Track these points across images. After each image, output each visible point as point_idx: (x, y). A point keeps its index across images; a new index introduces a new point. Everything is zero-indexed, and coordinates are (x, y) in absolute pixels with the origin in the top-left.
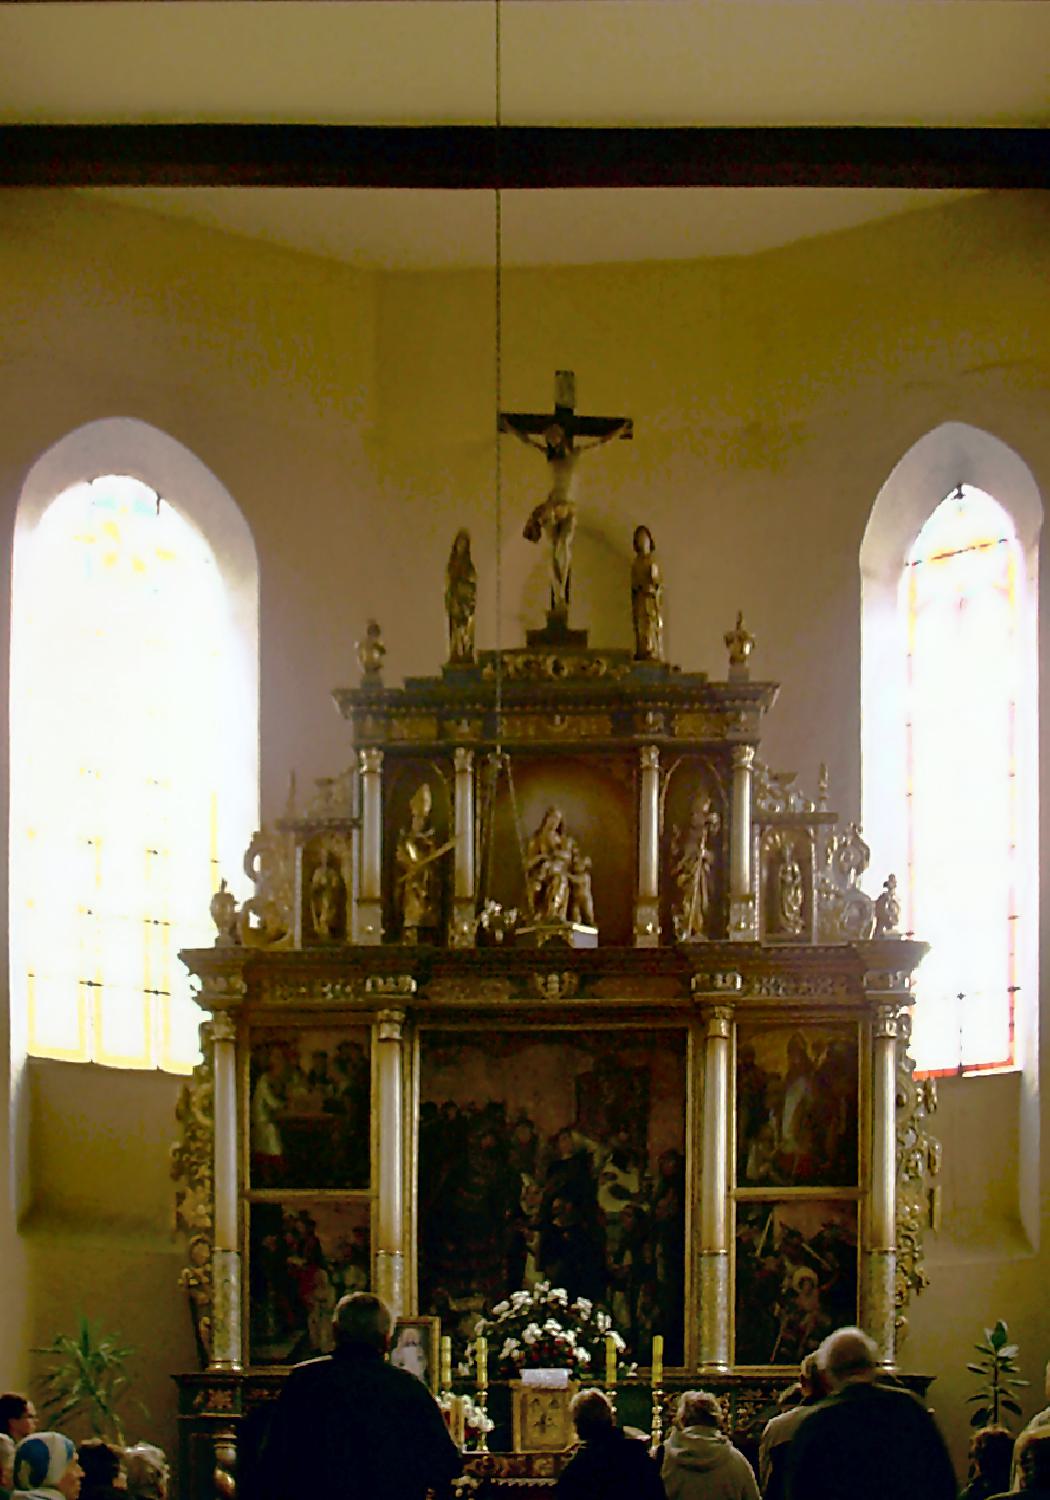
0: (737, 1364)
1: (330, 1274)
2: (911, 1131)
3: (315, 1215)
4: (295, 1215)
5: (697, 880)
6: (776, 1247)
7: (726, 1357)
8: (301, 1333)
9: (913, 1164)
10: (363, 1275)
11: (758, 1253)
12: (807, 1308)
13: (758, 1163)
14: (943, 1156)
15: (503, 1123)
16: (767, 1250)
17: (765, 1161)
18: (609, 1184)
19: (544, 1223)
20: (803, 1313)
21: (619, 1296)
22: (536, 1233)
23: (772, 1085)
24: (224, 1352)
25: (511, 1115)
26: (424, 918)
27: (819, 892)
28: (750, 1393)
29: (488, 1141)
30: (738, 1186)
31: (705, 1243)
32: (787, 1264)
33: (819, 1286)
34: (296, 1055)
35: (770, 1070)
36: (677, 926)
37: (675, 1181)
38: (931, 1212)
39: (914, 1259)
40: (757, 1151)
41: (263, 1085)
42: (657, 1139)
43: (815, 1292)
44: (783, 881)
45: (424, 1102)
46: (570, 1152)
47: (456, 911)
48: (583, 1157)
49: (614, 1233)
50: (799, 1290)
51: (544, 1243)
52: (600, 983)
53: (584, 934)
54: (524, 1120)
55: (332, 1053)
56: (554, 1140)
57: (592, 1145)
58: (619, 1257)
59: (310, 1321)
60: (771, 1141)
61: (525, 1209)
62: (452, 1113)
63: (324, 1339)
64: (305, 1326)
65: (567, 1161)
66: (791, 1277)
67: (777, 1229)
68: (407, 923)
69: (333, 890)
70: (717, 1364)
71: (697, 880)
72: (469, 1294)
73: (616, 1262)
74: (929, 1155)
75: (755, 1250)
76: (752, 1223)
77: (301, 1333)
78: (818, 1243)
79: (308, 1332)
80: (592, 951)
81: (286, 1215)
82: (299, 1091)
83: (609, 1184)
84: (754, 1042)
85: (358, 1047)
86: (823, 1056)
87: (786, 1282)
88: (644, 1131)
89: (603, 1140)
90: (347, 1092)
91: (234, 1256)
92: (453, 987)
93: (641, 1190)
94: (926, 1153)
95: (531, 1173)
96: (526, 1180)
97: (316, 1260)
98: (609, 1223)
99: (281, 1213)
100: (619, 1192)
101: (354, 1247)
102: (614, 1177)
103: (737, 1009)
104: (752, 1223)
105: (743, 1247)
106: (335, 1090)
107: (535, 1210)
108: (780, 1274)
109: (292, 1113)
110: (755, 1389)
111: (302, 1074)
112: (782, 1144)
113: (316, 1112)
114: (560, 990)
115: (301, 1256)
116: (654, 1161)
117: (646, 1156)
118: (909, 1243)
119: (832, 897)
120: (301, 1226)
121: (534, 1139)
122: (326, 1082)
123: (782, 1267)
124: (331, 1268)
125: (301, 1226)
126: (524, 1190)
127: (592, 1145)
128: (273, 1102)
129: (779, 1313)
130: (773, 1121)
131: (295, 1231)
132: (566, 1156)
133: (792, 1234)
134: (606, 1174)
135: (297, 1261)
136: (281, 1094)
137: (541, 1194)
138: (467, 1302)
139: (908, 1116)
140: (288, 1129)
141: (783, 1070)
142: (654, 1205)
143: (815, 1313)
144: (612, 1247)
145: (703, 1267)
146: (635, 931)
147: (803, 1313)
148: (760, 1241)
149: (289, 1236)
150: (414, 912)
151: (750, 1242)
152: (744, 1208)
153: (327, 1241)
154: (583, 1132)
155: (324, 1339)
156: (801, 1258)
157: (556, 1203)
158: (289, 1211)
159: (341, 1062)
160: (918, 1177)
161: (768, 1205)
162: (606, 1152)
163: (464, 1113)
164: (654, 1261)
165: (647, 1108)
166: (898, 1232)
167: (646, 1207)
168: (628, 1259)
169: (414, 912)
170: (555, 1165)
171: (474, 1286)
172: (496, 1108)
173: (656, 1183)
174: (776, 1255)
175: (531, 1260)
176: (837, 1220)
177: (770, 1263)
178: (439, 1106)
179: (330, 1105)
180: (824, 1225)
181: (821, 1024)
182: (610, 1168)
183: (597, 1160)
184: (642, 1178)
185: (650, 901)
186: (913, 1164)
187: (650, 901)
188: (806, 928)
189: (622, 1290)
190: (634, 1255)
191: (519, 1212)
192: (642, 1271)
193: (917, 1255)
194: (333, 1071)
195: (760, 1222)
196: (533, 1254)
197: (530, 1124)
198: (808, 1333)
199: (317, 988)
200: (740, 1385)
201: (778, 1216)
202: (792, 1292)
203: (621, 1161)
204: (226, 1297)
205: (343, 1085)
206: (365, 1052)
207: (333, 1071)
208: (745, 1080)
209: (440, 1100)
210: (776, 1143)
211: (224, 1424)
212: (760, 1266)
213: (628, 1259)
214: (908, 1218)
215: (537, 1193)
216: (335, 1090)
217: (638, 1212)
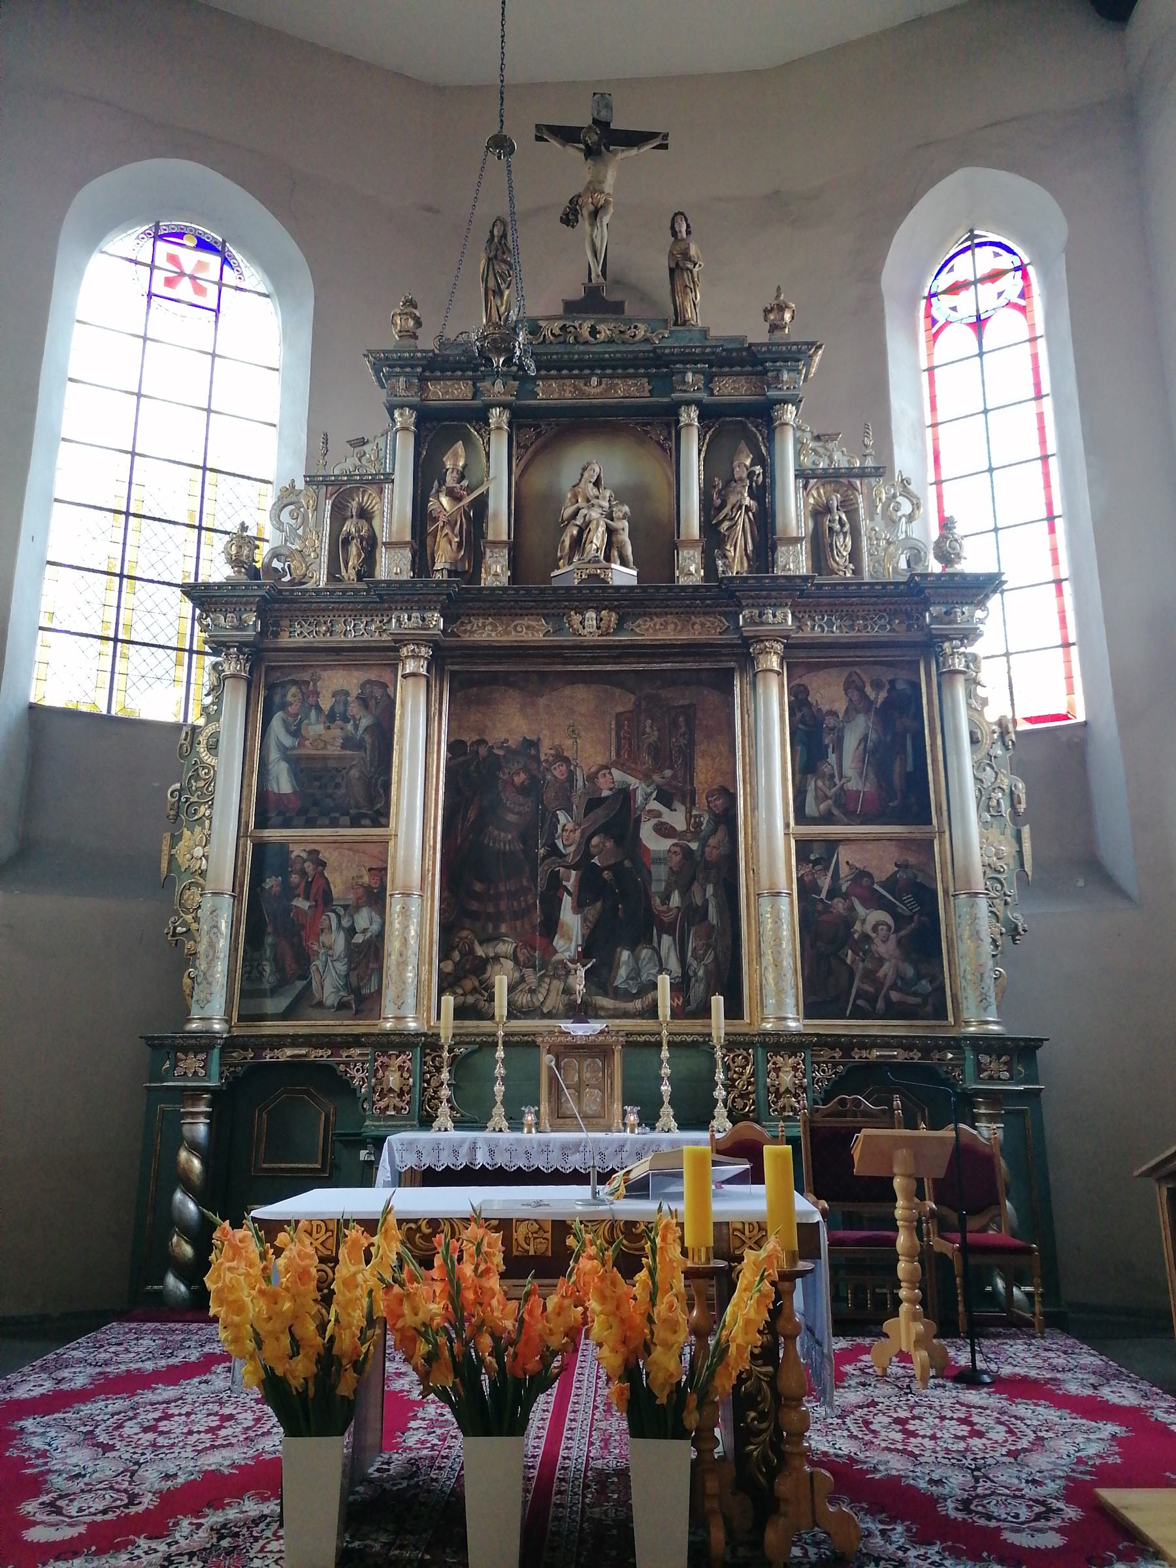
0: (807, 1017)
1: (339, 917)
2: (988, 768)
3: (325, 855)
4: (304, 855)
5: (740, 527)
6: (844, 888)
7: (794, 1010)
8: (300, 984)
9: (994, 803)
10: (377, 918)
11: (823, 896)
12: (886, 956)
13: (819, 799)
14: (1027, 794)
15: (536, 758)
16: (833, 893)
17: (826, 797)
18: (654, 821)
19: (584, 863)
20: (881, 961)
21: (666, 940)
22: (573, 873)
23: (829, 721)
24: (202, 1008)
25: (545, 751)
26: (454, 563)
27: (870, 538)
28: (825, 1054)
29: (521, 778)
30: (797, 823)
31: (765, 882)
32: (860, 909)
33: (897, 931)
34: (317, 694)
35: (825, 708)
36: (720, 569)
37: (726, 819)
38: (1020, 853)
39: (1006, 903)
40: (816, 787)
41: (277, 722)
42: (704, 775)
43: (893, 937)
44: (831, 529)
45: (452, 739)
46: (611, 789)
47: (488, 553)
48: (625, 795)
49: (660, 873)
50: (873, 935)
51: (582, 883)
52: (640, 621)
53: (623, 575)
54: (560, 757)
55: (355, 692)
56: (592, 778)
57: (634, 782)
58: (666, 898)
59: (313, 968)
60: (832, 776)
61: (561, 847)
62: (483, 751)
63: (328, 989)
64: (304, 975)
65: (607, 798)
66: (864, 921)
67: (844, 871)
68: (438, 566)
69: (362, 538)
70: (785, 1019)
71: (740, 527)
72: (496, 938)
73: (663, 903)
74: (1012, 792)
75: (819, 892)
76: (816, 862)
77: (300, 984)
78: (891, 884)
79: (310, 983)
80: (631, 588)
81: (293, 855)
82: (315, 728)
83: (654, 821)
84: (805, 680)
85: (384, 686)
86: (883, 695)
87: (857, 926)
88: (689, 767)
89: (646, 777)
90: (366, 729)
91: (226, 902)
92: (484, 626)
93: (688, 828)
94: (1007, 791)
95: (569, 810)
96: (562, 817)
97: (325, 899)
98: (659, 861)
99: (290, 852)
100: (664, 830)
101: (368, 889)
102: (659, 814)
103: (786, 646)
104: (816, 862)
105: (806, 889)
106: (356, 727)
107: (572, 849)
108: (848, 921)
109: (308, 750)
110: (833, 1049)
111: (319, 709)
112: (843, 780)
113: (334, 750)
114: (598, 628)
115: (307, 898)
116: (701, 799)
117: (693, 792)
118: (999, 887)
119: (883, 543)
120: (309, 867)
121: (571, 775)
122: (346, 720)
123: (852, 909)
124: (342, 912)
125: (309, 867)
126: (560, 828)
127: (634, 782)
128: (288, 741)
129: (853, 961)
130: (832, 758)
131: (303, 873)
132: (605, 793)
133: (861, 875)
134: (650, 811)
135: (302, 904)
136: (296, 733)
137: (578, 833)
138: (494, 948)
139: (984, 753)
140: (299, 766)
141: (841, 706)
142: (704, 844)
143: (894, 961)
144: (657, 887)
145: (762, 910)
146: (677, 573)
147: (881, 961)
148: (825, 883)
149: (295, 878)
150: (444, 556)
151: (814, 882)
152: (804, 847)
153: (338, 883)
154: (622, 767)
155: (328, 989)
156: (875, 901)
157: (595, 841)
158: (297, 851)
159: (363, 701)
160: (1002, 815)
161: (832, 845)
162: (649, 790)
163: (496, 751)
164: (706, 902)
165: (691, 743)
166: (985, 873)
167: (694, 846)
168: (675, 900)
169: (444, 556)
170: (594, 803)
171: (503, 928)
172: (532, 744)
173: (705, 819)
174: (846, 896)
175: (567, 901)
176: (912, 860)
177: (839, 905)
178: (468, 744)
179: (348, 743)
180: (896, 865)
181: (875, 663)
182: (654, 805)
183: (640, 799)
184: (689, 816)
185: (691, 544)
186: (994, 803)
187: (691, 544)
188: (857, 572)
189: (671, 933)
190: (683, 895)
191: (554, 851)
192: (694, 914)
193: (1009, 899)
194: (354, 709)
195: (823, 862)
196: (569, 893)
197: (567, 760)
198: (888, 983)
199: (339, 627)
200: (815, 1045)
201: (844, 854)
202: (866, 938)
203: (666, 798)
204: (212, 945)
205: (365, 722)
206: (390, 691)
207: (354, 709)
208: (799, 715)
209: (469, 738)
210: (836, 780)
211: (194, 1094)
212: (827, 909)
213: (675, 900)
214: (995, 859)
215: (574, 831)
216: (356, 727)
217: (688, 853)
